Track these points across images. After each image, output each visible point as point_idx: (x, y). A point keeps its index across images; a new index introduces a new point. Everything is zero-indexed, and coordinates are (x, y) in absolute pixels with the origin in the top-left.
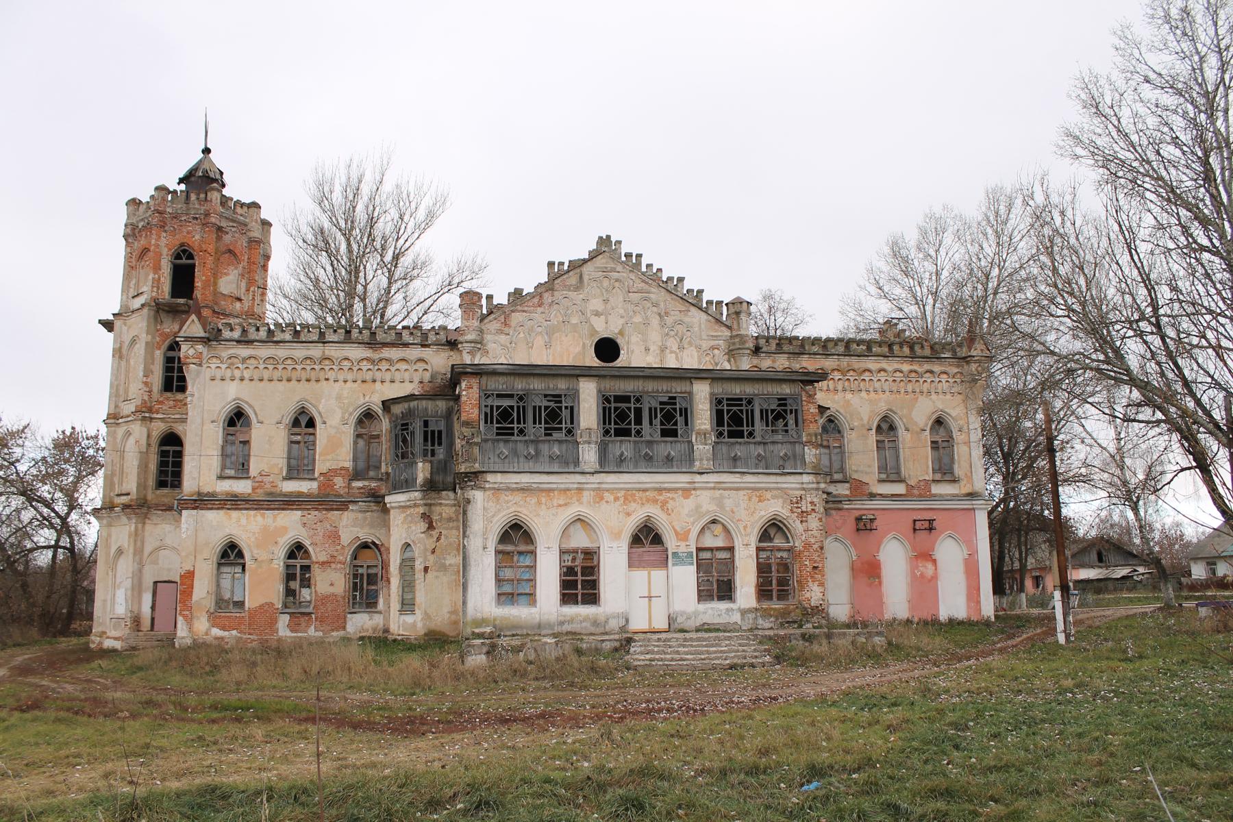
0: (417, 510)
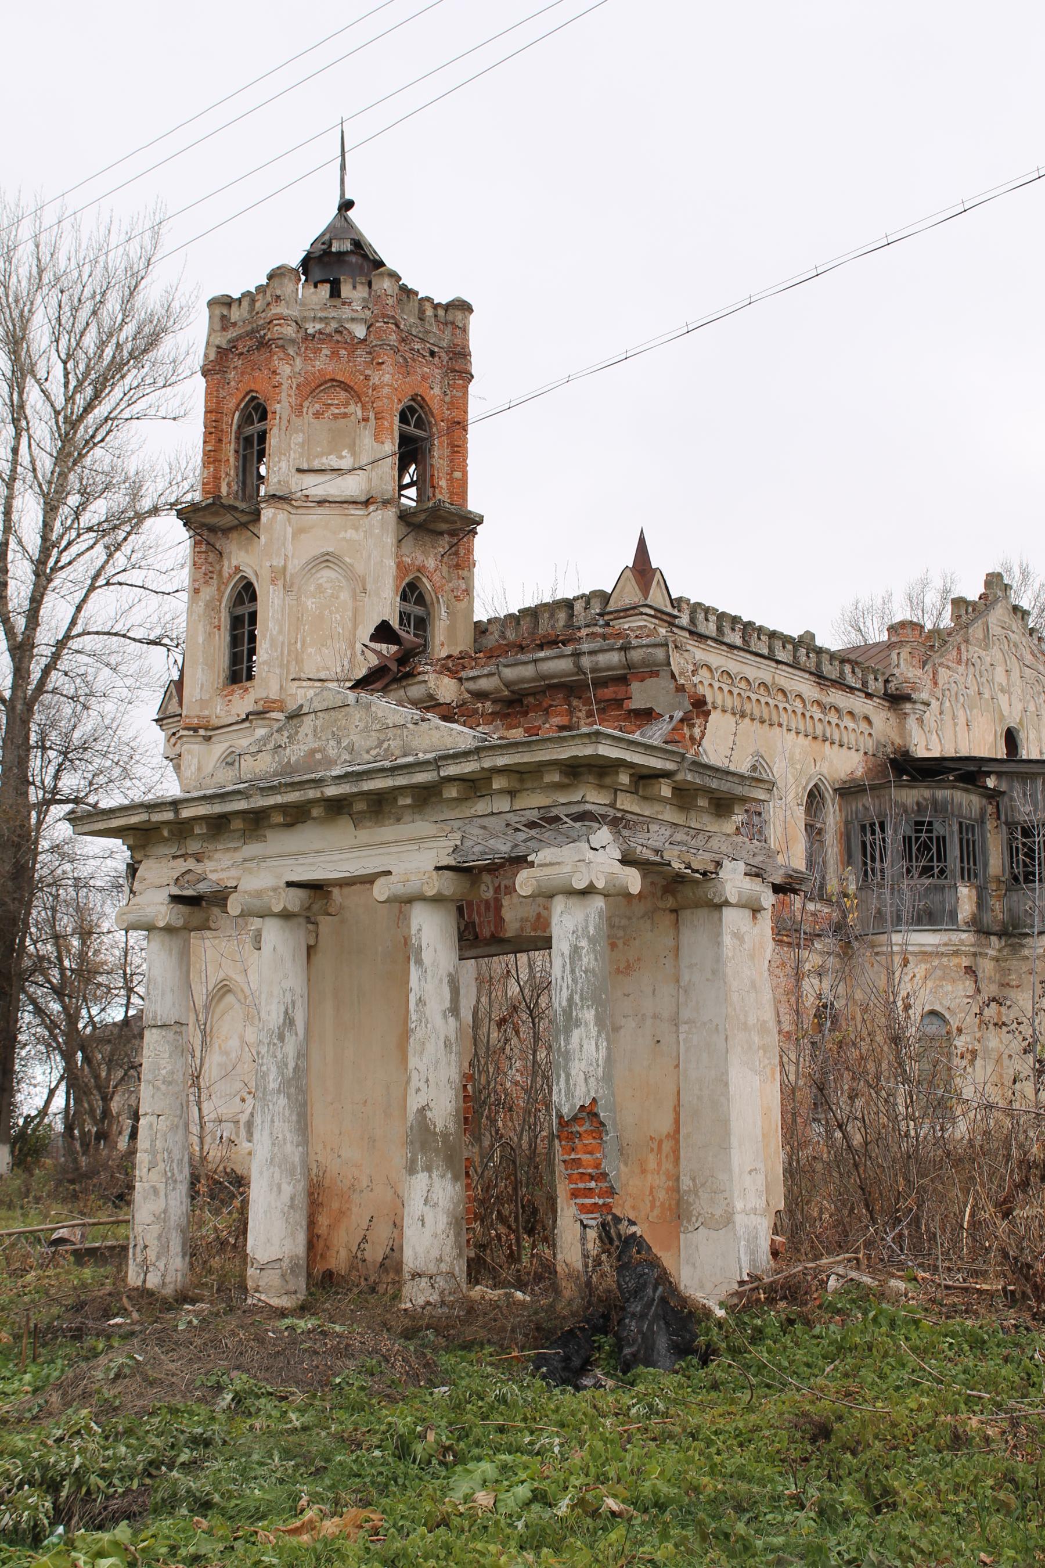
0: (955, 960)
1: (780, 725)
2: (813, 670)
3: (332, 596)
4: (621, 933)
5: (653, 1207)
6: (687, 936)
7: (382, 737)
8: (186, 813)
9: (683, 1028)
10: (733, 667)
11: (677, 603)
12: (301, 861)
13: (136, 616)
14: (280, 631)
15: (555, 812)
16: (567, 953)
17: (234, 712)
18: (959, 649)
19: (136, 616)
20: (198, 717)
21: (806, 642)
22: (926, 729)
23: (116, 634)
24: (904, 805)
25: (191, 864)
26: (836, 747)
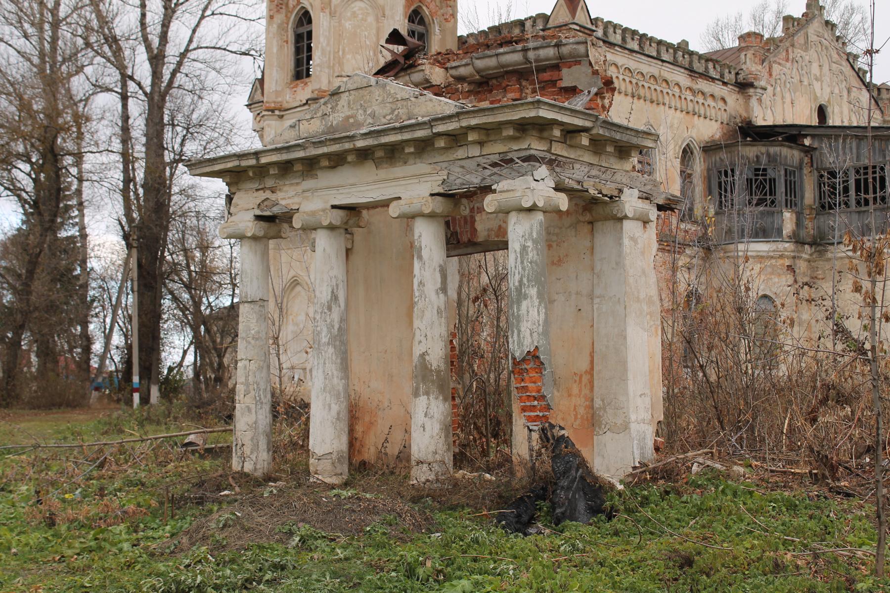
0: (781, 262)
1: (664, 104)
2: (687, 66)
3: (362, 19)
4: (555, 238)
5: (576, 418)
6: (599, 240)
7: (394, 107)
8: (264, 160)
9: (596, 301)
10: (632, 65)
11: (595, 21)
12: (341, 191)
13: (232, 36)
14: (328, 44)
15: (510, 156)
16: (518, 250)
17: (298, 98)
18: (787, 51)
19: (232, 36)
20: (275, 102)
21: (682, 47)
22: (764, 106)
23: (219, 48)
24: (748, 158)
25: (268, 194)
26: (702, 118)
